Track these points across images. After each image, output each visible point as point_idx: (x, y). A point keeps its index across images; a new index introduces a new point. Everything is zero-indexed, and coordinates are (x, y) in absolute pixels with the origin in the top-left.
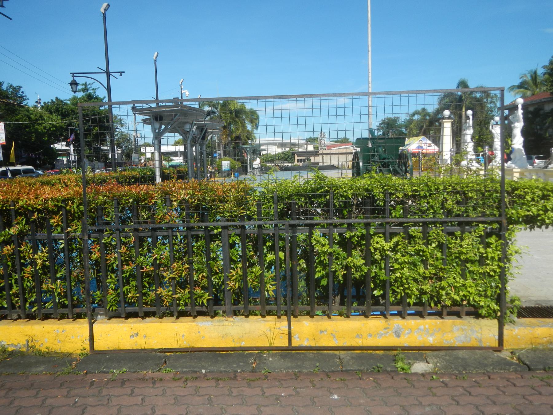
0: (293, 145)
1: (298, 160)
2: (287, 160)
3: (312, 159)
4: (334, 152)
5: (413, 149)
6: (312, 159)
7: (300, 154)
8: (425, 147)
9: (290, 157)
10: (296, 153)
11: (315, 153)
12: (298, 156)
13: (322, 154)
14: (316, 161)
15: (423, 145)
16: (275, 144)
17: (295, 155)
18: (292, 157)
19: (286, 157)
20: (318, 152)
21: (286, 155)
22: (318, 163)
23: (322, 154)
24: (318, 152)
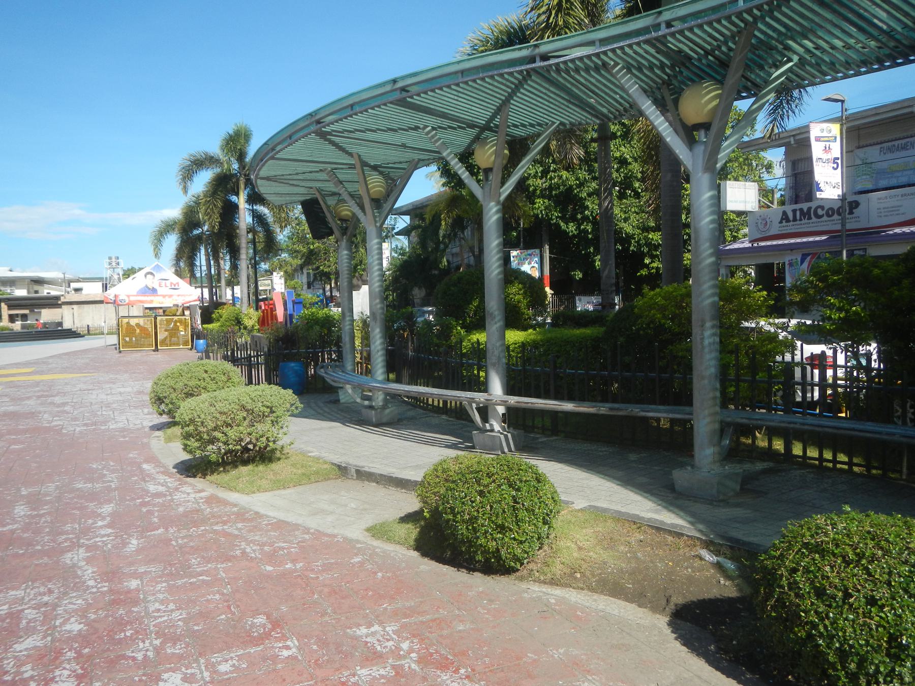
0: (39, 282)
3: (47, 316)
5: (128, 296)
6: (47, 316)
8: (160, 291)
11: (53, 302)
12: (10, 307)
14: (58, 320)
15: (157, 287)
22: (60, 324)
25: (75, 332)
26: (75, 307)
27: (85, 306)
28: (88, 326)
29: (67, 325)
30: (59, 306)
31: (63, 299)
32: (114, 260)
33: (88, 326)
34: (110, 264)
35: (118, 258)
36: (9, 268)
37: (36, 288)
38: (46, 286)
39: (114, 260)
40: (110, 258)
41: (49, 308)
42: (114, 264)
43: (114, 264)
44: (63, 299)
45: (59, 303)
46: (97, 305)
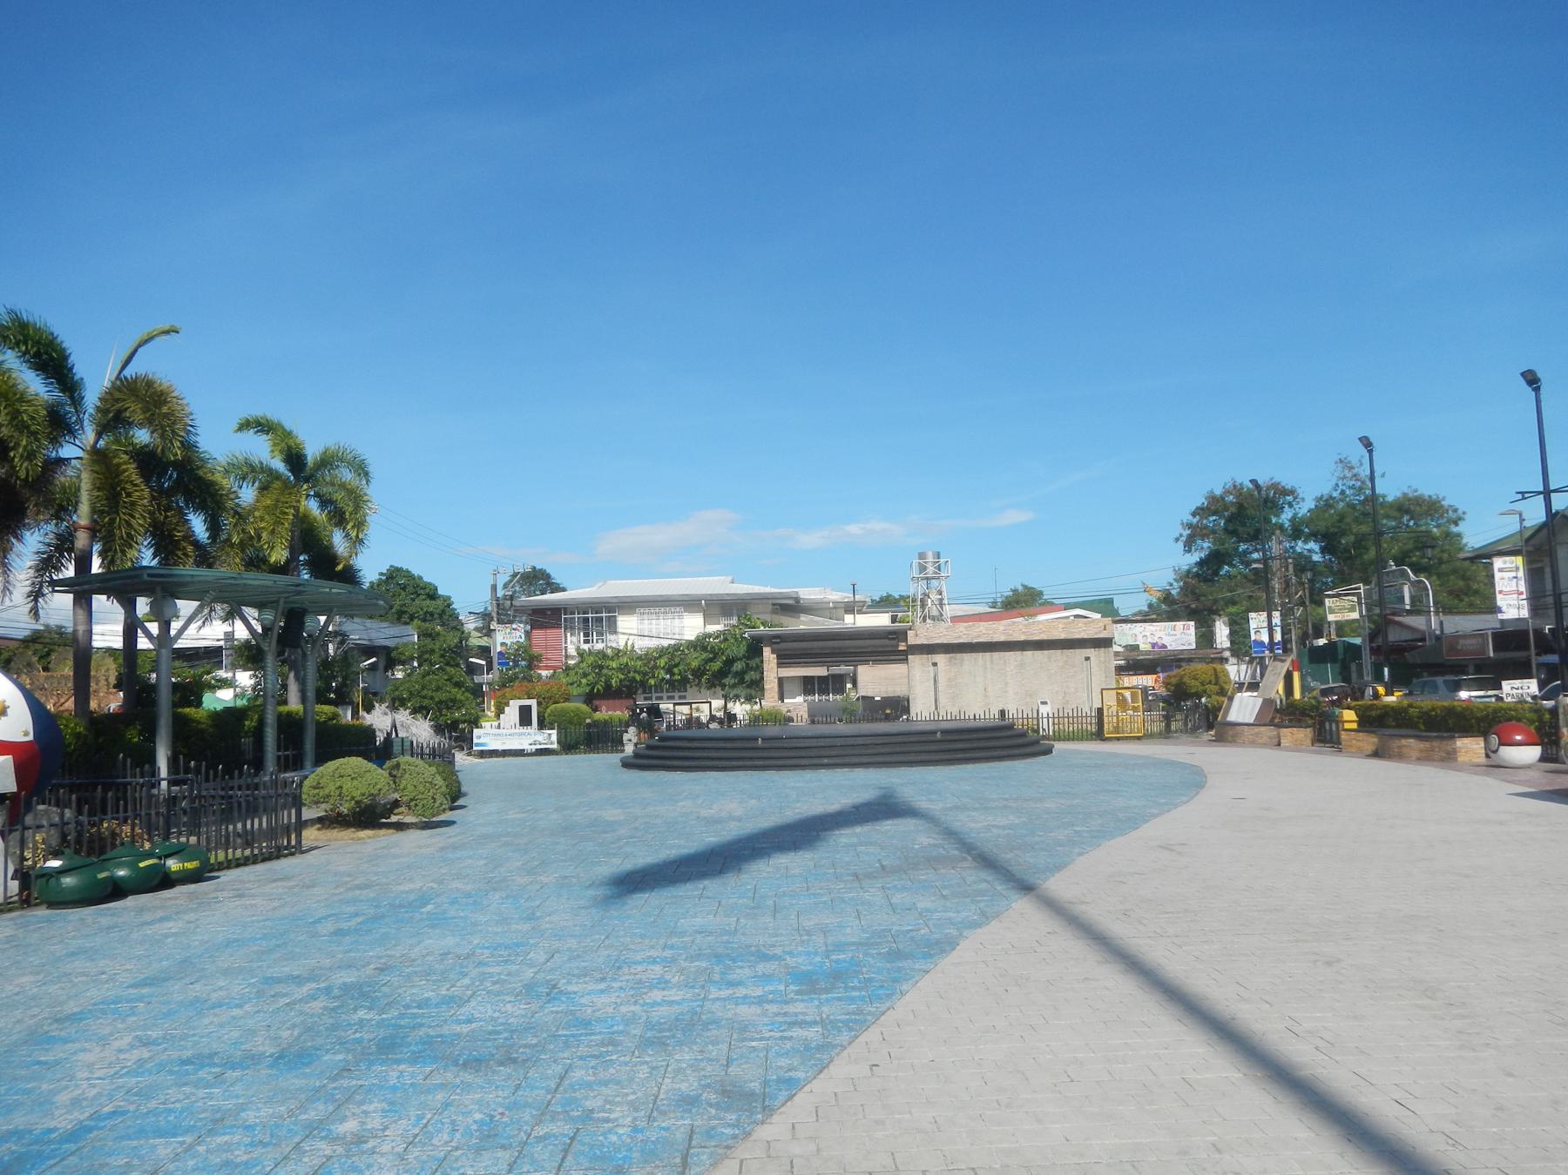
1: (781, 681)
2: (723, 686)
3: (874, 680)
4: (1002, 638)
6: (874, 680)
7: (794, 650)
9: (738, 666)
10: (775, 640)
12: (784, 659)
13: (929, 649)
14: (897, 690)
16: (689, 604)
17: (767, 651)
18: (748, 668)
19: (716, 665)
20: (901, 635)
21: (715, 654)
23: (929, 649)
24: (901, 635)
25: (1023, 735)
26: (941, 659)
27: (968, 658)
28: (1002, 713)
29: (922, 710)
30: (901, 657)
31: (912, 639)
32: (930, 558)
33: (1002, 713)
34: (923, 568)
35: (938, 555)
36: (730, 578)
37: (785, 620)
38: (803, 617)
39: (930, 558)
40: (922, 556)
41: (876, 662)
42: (931, 569)
43: (931, 569)
44: (912, 639)
45: (902, 647)
46: (996, 655)
